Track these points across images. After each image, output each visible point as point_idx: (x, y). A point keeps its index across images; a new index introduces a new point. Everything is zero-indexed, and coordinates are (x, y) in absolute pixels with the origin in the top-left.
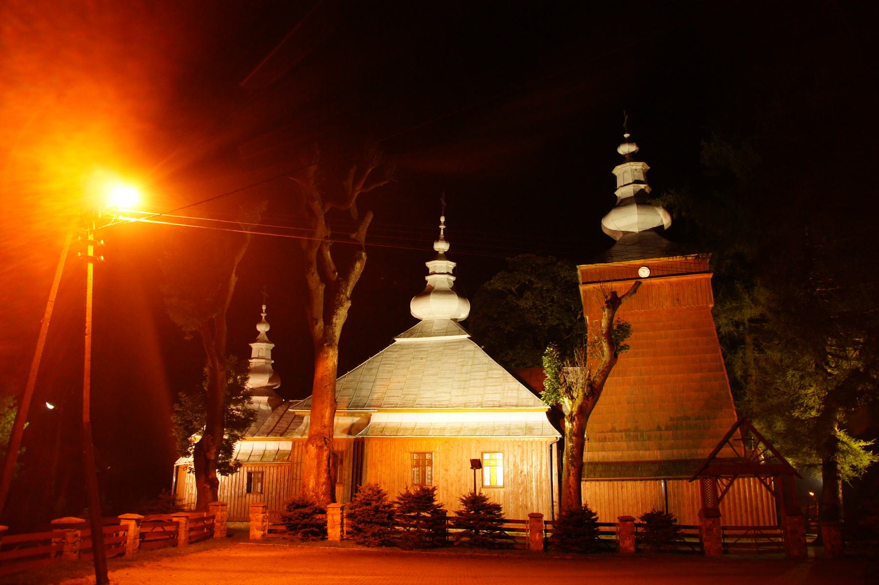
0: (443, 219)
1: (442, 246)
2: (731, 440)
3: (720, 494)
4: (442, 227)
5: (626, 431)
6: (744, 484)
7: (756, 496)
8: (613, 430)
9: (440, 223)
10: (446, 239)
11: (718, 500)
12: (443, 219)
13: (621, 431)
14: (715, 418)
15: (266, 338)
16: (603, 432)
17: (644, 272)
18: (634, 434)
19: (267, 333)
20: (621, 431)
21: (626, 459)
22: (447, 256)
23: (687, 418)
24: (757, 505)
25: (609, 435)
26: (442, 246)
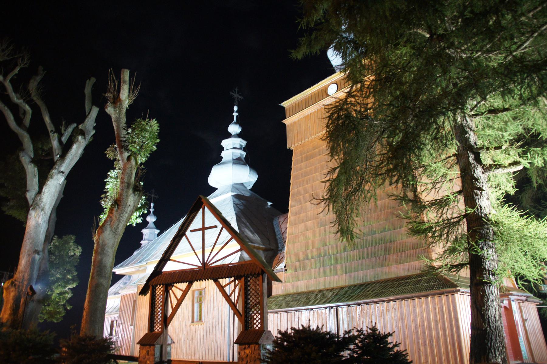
0: (236, 108)
1: (234, 129)
2: (188, 233)
3: (170, 311)
4: (235, 114)
5: (318, 257)
6: (421, 306)
7: (436, 322)
8: (306, 258)
9: (233, 111)
10: (238, 122)
11: (166, 321)
12: (236, 108)
13: (313, 258)
14: (401, 228)
15: (153, 226)
16: (298, 261)
17: (332, 90)
18: (323, 258)
19: (155, 223)
20: (313, 258)
21: (315, 288)
22: (239, 136)
23: (373, 233)
24: (438, 333)
25: (303, 263)
26: (234, 129)
